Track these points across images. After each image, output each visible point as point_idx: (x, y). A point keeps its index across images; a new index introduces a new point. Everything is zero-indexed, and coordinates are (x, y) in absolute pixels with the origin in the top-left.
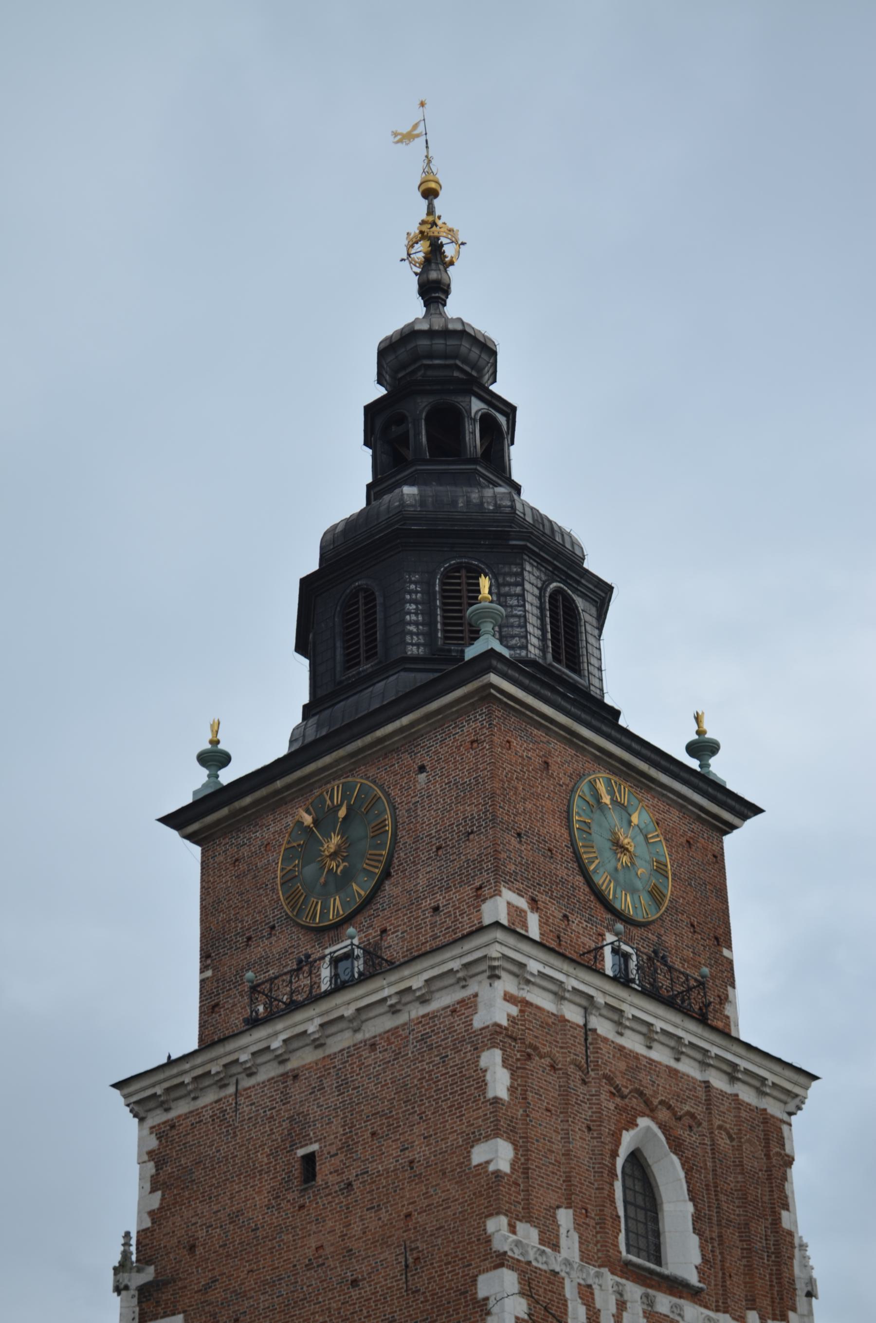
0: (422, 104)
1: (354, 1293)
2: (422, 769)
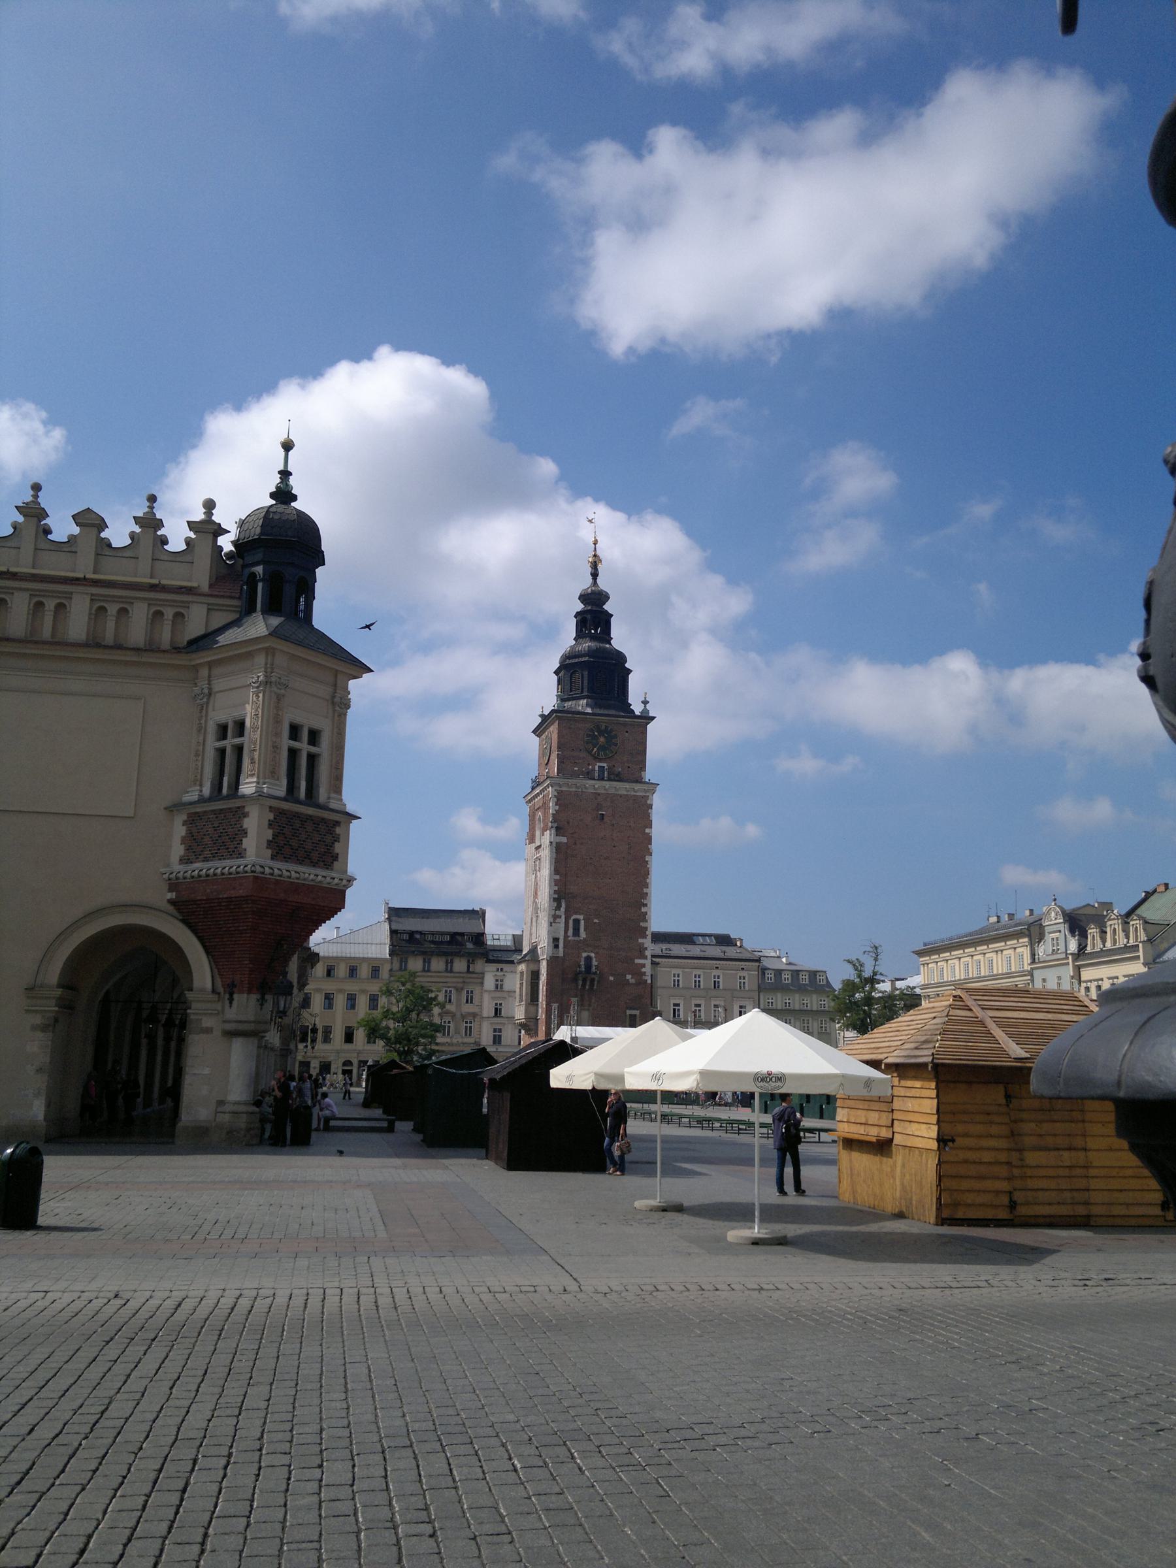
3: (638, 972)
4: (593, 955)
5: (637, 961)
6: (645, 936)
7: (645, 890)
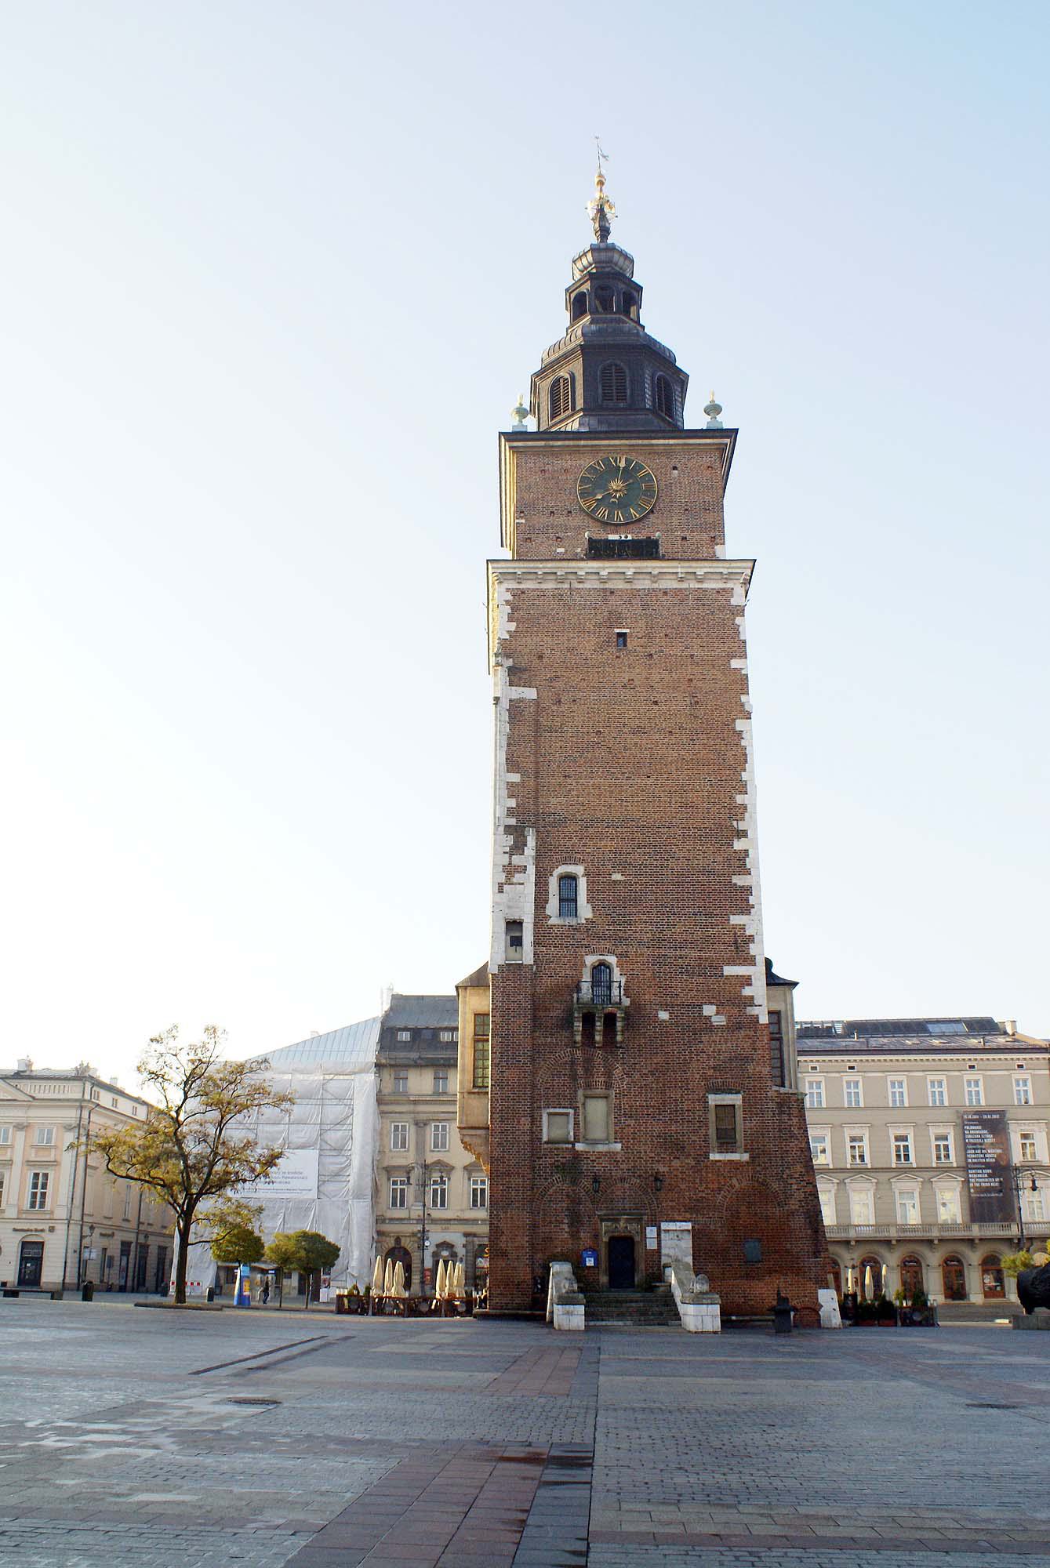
1: (656, 708)
2: (675, 468)
3: (734, 1000)
4: (612, 960)
5: (729, 970)
7: (740, 799)
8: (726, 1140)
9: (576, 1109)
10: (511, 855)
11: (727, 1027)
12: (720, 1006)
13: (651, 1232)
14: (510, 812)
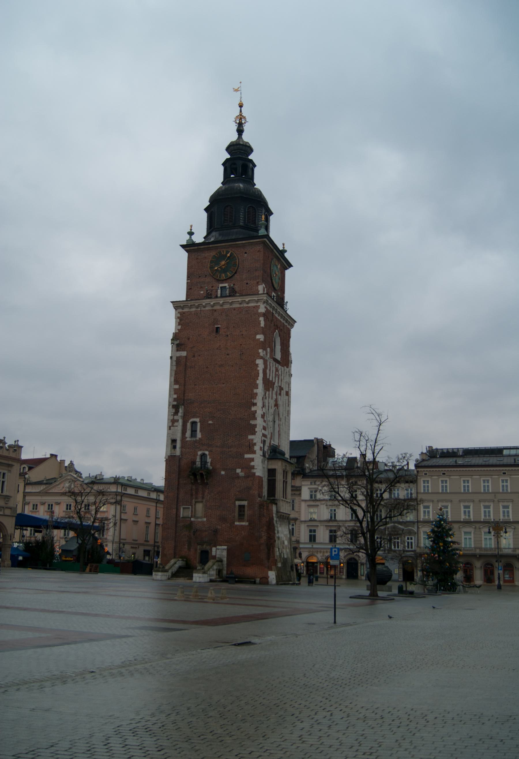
0: (241, 83)
1: (228, 357)
2: (246, 253)
3: (248, 467)
4: (207, 453)
5: (247, 456)
6: (254, 433)
7: (255, 391)
8: (241, 517)
9: (192, 506)
10: (174, 415)
11: (244, 477)
12: (242, 469)
13: (214, 549)
14: (175, 400)
